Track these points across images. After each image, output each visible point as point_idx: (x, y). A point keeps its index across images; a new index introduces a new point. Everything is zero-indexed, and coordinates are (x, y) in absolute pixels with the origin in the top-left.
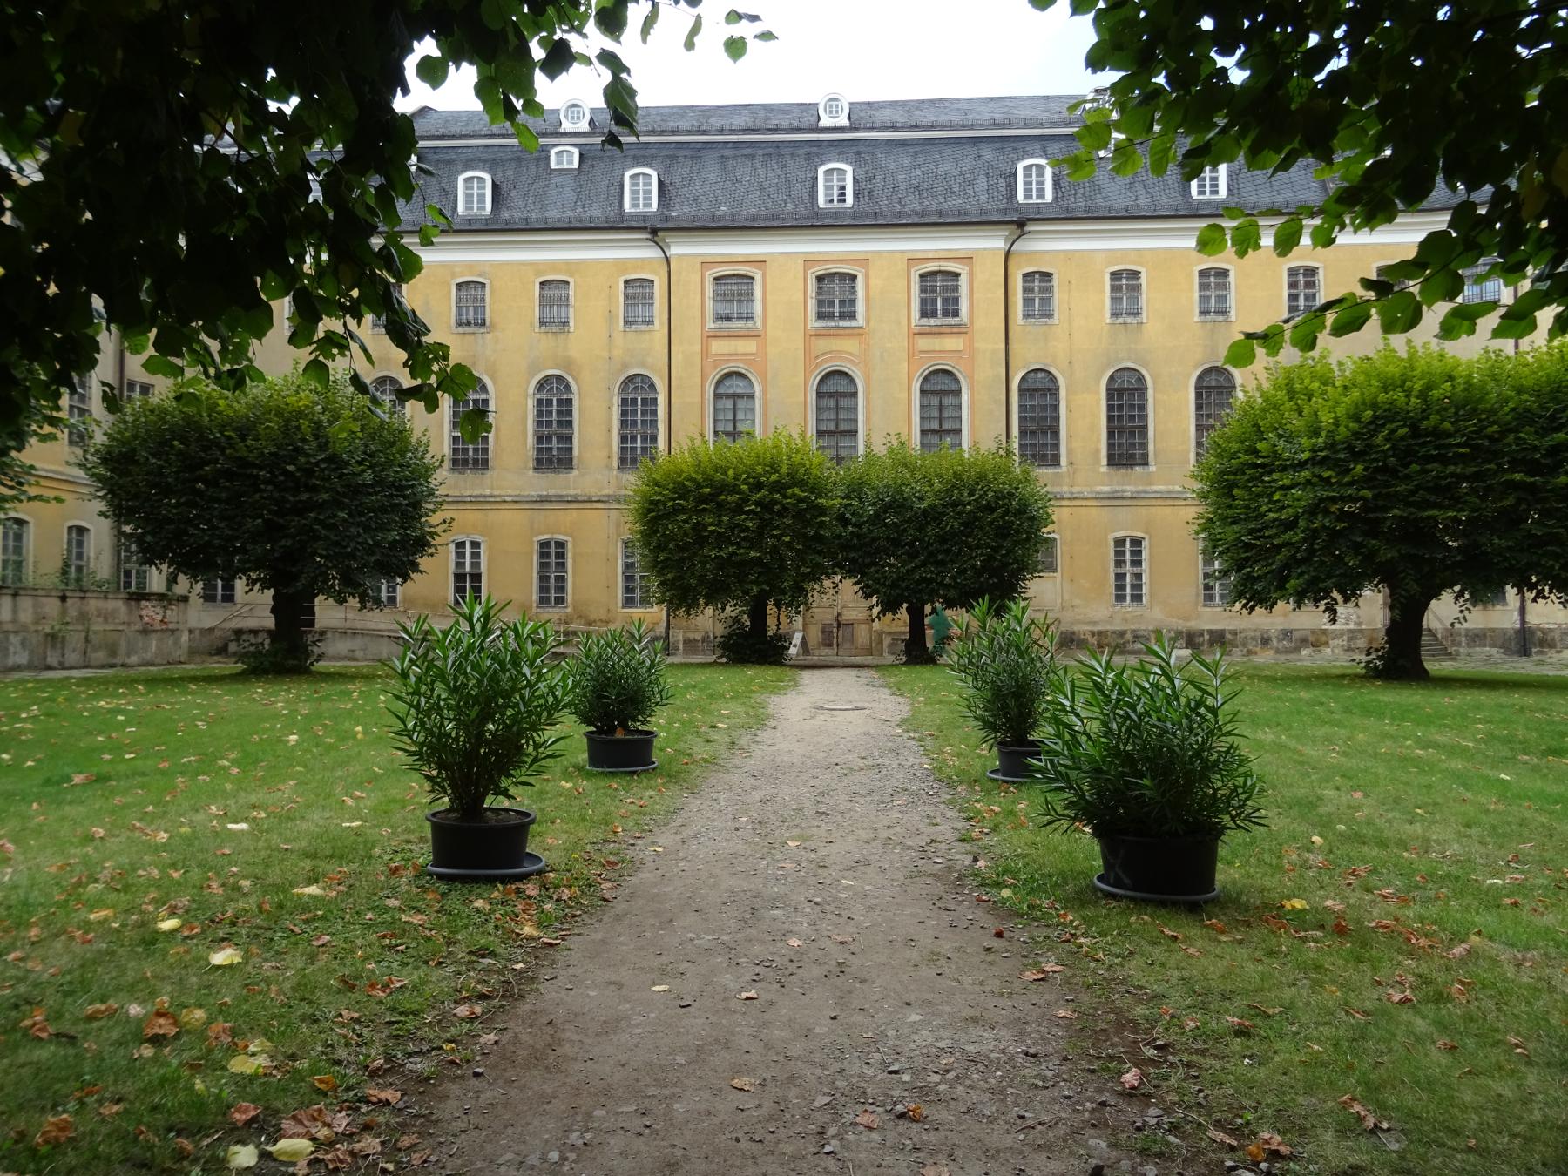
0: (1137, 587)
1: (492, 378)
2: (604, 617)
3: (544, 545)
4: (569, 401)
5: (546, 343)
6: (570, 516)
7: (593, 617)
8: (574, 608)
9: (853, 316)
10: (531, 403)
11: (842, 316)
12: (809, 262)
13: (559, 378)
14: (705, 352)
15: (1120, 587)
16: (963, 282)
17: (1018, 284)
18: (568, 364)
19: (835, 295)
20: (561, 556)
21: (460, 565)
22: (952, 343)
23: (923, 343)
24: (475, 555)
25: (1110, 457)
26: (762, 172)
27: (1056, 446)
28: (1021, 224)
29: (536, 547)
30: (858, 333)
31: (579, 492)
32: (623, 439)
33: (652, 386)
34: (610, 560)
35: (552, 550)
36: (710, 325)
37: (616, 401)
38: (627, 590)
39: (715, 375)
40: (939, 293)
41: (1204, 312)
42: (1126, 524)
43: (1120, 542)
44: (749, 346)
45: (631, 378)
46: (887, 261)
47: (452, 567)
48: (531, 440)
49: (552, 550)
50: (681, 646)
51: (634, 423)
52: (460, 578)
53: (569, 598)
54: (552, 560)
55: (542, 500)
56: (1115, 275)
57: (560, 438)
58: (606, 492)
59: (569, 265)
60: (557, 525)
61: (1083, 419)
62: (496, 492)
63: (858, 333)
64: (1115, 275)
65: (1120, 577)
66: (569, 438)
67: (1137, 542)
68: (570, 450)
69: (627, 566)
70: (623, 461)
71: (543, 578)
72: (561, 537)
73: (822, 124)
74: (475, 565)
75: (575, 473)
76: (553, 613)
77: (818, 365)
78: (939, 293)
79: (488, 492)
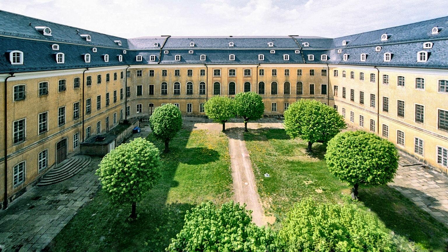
0: (275, 109)
5: (189, 78)
6: (192, 100)
12: (228, 68)
14: (213, 79)
15: (273, 109)
16: (251, 71)
17: (259, 71)
18: (192, 81)
19: (232, 72)
22: (249, 79)
23: (245, 79)
25: (272, 93)
27: (264, 91)
28: (260, 64)
36: (213, 76)
40: (247, 72)
41: (285, 75)
42: (274, 101)
43: (273, 104)
44: (219, 79)
46: (240, 68)
48: (186, 91)
53: (192, 111)
55: (188, 98)
56: (273, 70)
59: (192, 68)
61: (268, 88)
64: (273, 70)
65: (273, 108)
67: (275, 104)
70: (200, 93)
76: (189, 113)
78: (247, 72)
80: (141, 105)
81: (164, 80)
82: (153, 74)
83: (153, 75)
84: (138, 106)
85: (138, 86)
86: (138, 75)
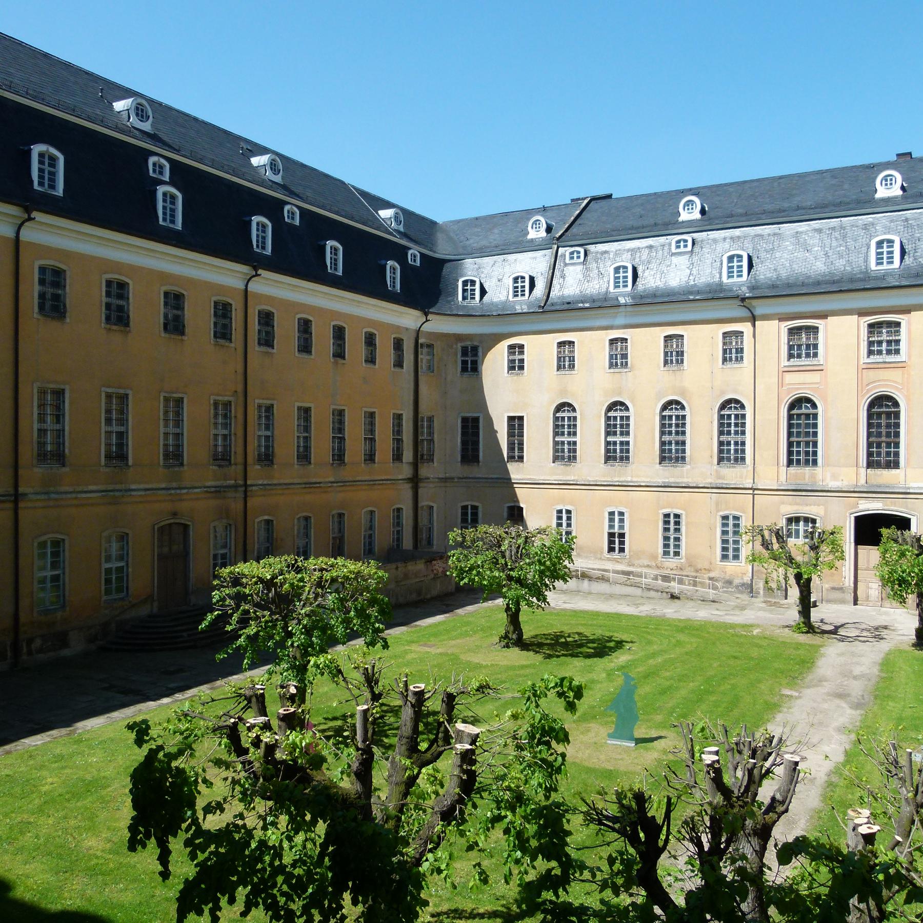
1: (632, 402)
2: (707, 567)
3: (667, 516)
4: (684, 417)
7: (699, 566)
8: (687, 559)
9: (897, 352)
10: (657, 418)
11: (889, 352)
13: (677, 403)
14: (781, 384)
18: (683, 392)
20: (677, 523)
21: (611, 527)
24: (621, 521)
26: (827, 242)
29: (661, 517)
30: (902, 366)
31: (690, 480)
32: (721, 443)
33: (743, 407)
34: (712, 529)
35: (672, 520)
36: (785, 362)
37: (716, 417)
38: (725, 549)
39: (787, 399)
44: (814, 377)
45: (729, 401)
47: (606, 530)
49: (672, 520)
50: (762, 592)
51: (729, 433)
52: (611, 535)
53: (683, 551)
54: (672, 526)
57: (677, 443)
58: (709, 480)
60: (675, 503)
62: (634, 479)
63: (902, 366)
66: (684, 443)
68: (684, 451)
69: (725, 533)
71: (666, 539)
72: (677, 511)
73: (878, 195)
74: (621, 527)
75: (687, 467)
76: (671, 563)
77: (868, 391)
79: (629, 479)
80: (475, 508)
81: (563, 392)
82: (522, 361)
83: (521, 368)
84: (465, 508)
85: (465, 420)
86: (464, 369)
